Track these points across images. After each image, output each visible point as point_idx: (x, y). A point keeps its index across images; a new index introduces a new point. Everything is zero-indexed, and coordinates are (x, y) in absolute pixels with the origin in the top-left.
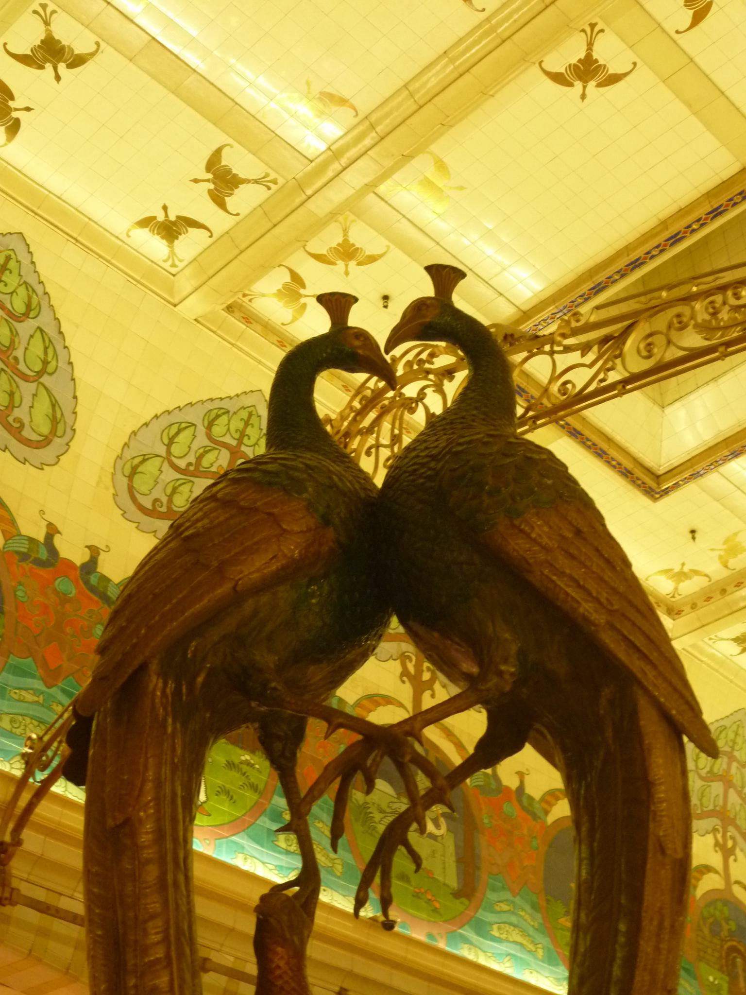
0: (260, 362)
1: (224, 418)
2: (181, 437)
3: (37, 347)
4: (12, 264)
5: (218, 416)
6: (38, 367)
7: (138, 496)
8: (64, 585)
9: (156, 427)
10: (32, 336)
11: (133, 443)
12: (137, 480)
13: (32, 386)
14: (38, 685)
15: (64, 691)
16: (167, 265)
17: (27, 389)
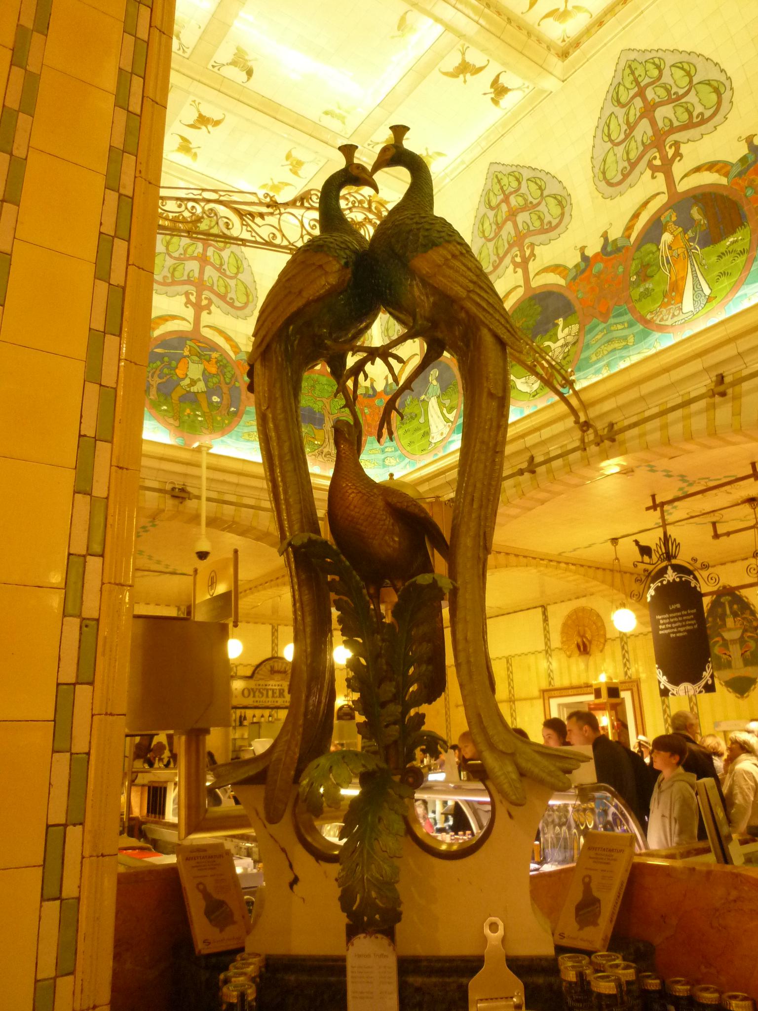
0: (605, 44)
1: (491, 194)
2: (612, 127)
3: (678, 73)
4: (500, 176)
5: (617, 93)
6: (687, 79)
7: (612, 181)
8: (599, 267)
9: (599, 141)
10: (672, 75)
11: (595, 163)
12: (608, 176)
13: (693, 92)
14: (603, 326)
15: (614, 317)
16: (527, 91)
17: (692, 98)
